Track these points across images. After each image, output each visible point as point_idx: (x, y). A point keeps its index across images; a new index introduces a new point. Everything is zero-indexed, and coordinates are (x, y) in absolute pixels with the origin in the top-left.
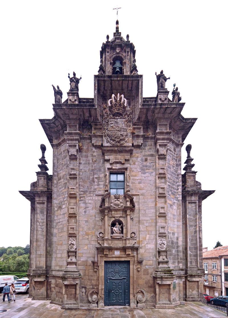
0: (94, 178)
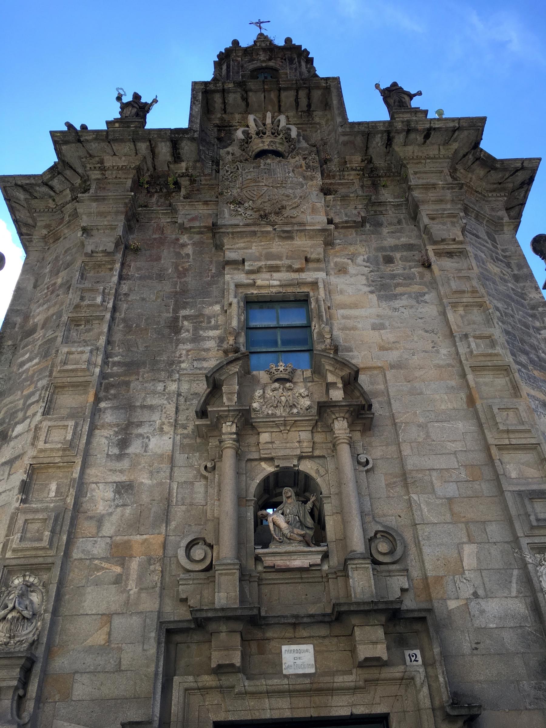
0: (176, 319)
